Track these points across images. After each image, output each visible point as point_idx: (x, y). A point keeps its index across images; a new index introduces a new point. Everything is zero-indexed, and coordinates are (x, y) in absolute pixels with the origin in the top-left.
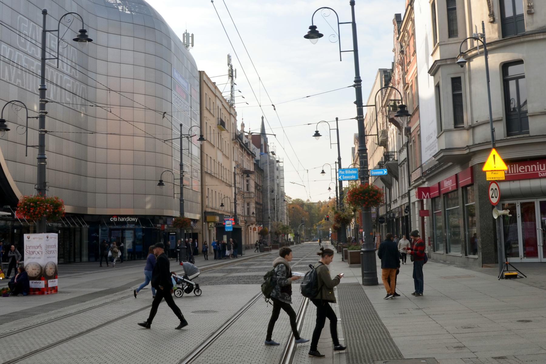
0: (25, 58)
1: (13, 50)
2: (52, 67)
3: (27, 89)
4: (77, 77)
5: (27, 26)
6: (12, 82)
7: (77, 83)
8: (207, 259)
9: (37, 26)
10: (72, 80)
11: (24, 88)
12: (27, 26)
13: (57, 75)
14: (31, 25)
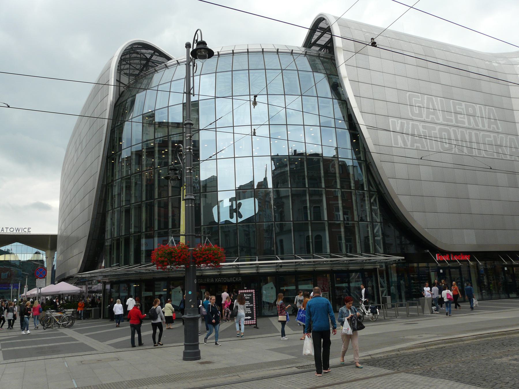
0: (423, 125)
1: (404, 121)
2: (461, 127)
3: (430, 150)
4: (500, 131)
5: (420, 99)
6: (409, 147)
7: (500, 135)
8: (140, 344)
9: (433, 97)
10: (492, 135)
11: (426, 149)
12: (420, 99)
13: (470, 134)
14: (426, 98)
